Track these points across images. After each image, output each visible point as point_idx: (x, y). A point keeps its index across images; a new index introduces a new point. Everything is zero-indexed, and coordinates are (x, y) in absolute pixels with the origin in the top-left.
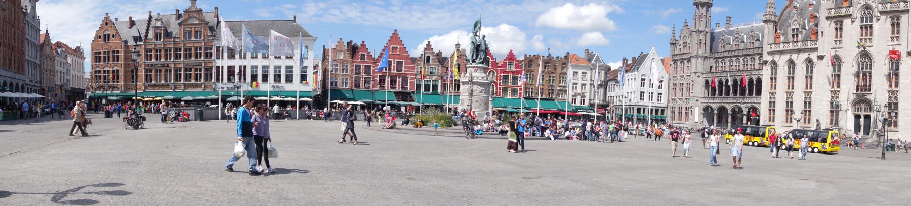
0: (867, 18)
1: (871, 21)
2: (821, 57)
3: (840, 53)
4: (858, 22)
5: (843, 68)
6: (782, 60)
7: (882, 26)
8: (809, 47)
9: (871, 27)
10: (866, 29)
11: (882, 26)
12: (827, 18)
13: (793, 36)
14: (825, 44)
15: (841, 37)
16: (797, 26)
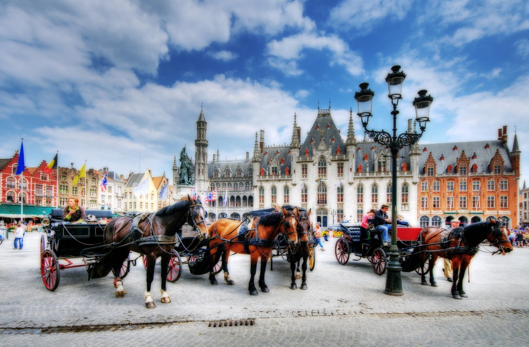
0: (322, 163)
1: (325, 165)
2: (295, 185)
3: (308, 183)
4: (317, 166)
5: (309, 191)
6: (268, 186)
7: (332, 168)
8: (286, 178)
9: (325, 168)
10: (323, 170)
11: (332, 168)
12: (297, 162)
13: (273, 171)
14: (297, 176)
15: (306, 173)
16: (276, 166)
